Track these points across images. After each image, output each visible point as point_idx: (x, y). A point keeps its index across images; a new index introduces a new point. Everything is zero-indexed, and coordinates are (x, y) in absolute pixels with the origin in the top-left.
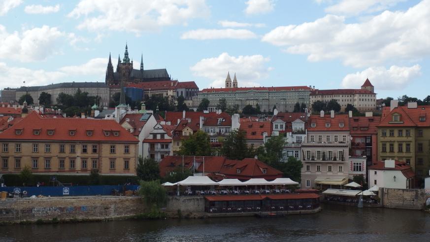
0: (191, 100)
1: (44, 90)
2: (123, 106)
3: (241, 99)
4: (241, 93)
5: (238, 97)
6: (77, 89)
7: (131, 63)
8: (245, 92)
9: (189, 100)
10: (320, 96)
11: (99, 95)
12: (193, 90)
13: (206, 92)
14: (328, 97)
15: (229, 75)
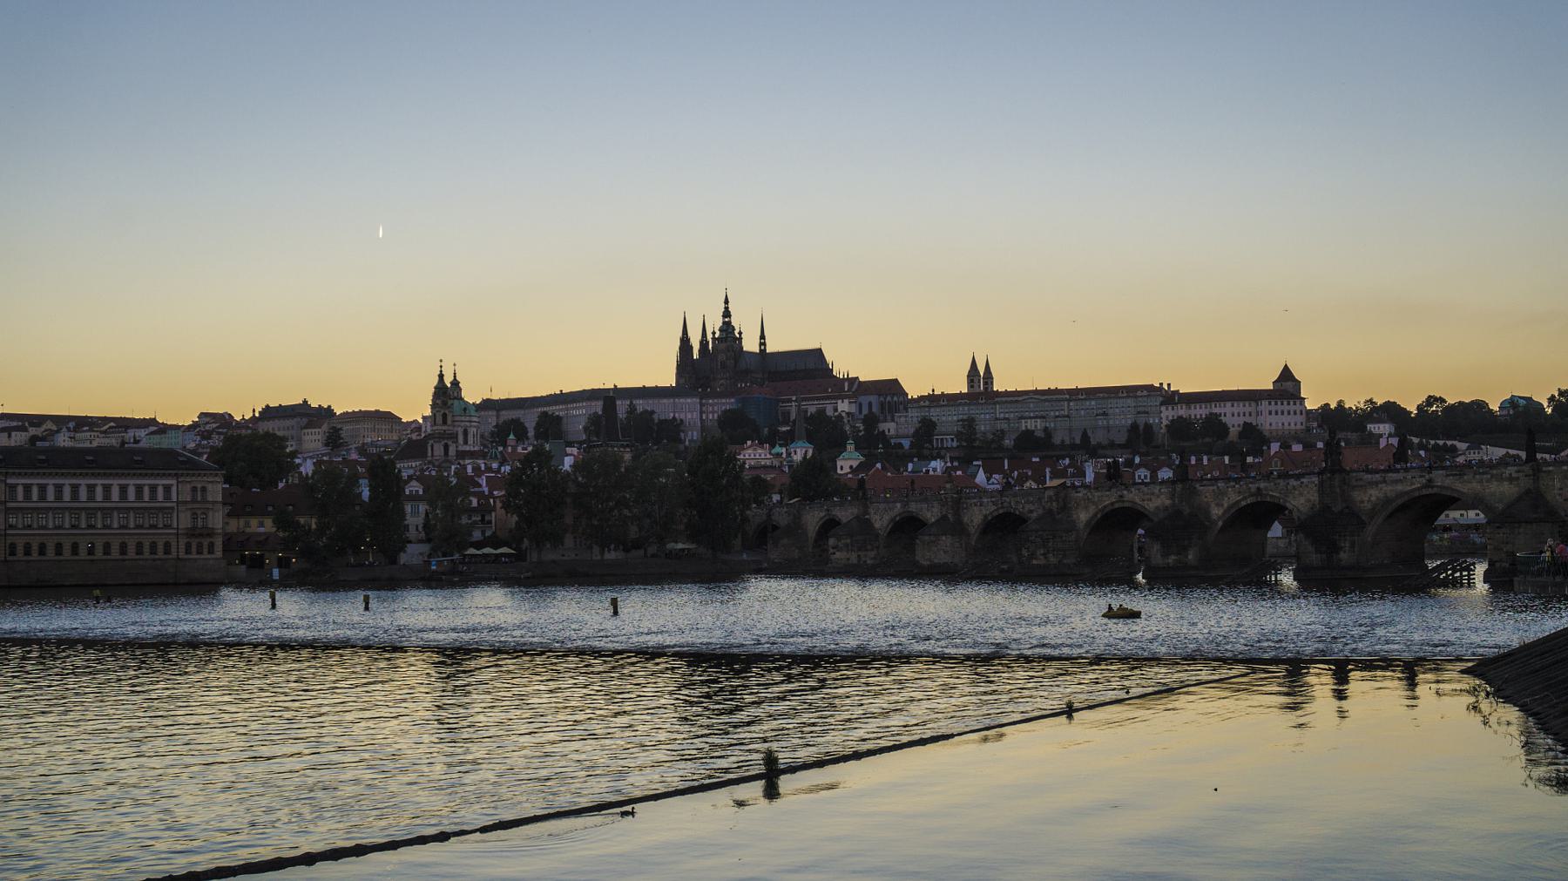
0: (893, 420)
1: (549, 405)
2: (805, 445)
3: (1007, 416)
4: (1006, 402)
5: (999, 411)
6: (628, 402)
7: (738, 336)
8: (1017, 401)
9: (885, 421)
10: (1184, 407)
11: (677, 415)
12: (895, 398)
13: (927, 403)
14: (1201, 408)
15: (974, 362)
